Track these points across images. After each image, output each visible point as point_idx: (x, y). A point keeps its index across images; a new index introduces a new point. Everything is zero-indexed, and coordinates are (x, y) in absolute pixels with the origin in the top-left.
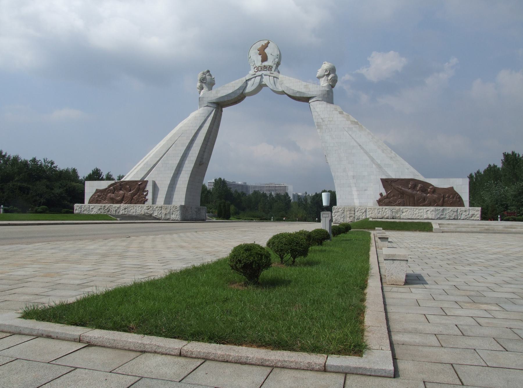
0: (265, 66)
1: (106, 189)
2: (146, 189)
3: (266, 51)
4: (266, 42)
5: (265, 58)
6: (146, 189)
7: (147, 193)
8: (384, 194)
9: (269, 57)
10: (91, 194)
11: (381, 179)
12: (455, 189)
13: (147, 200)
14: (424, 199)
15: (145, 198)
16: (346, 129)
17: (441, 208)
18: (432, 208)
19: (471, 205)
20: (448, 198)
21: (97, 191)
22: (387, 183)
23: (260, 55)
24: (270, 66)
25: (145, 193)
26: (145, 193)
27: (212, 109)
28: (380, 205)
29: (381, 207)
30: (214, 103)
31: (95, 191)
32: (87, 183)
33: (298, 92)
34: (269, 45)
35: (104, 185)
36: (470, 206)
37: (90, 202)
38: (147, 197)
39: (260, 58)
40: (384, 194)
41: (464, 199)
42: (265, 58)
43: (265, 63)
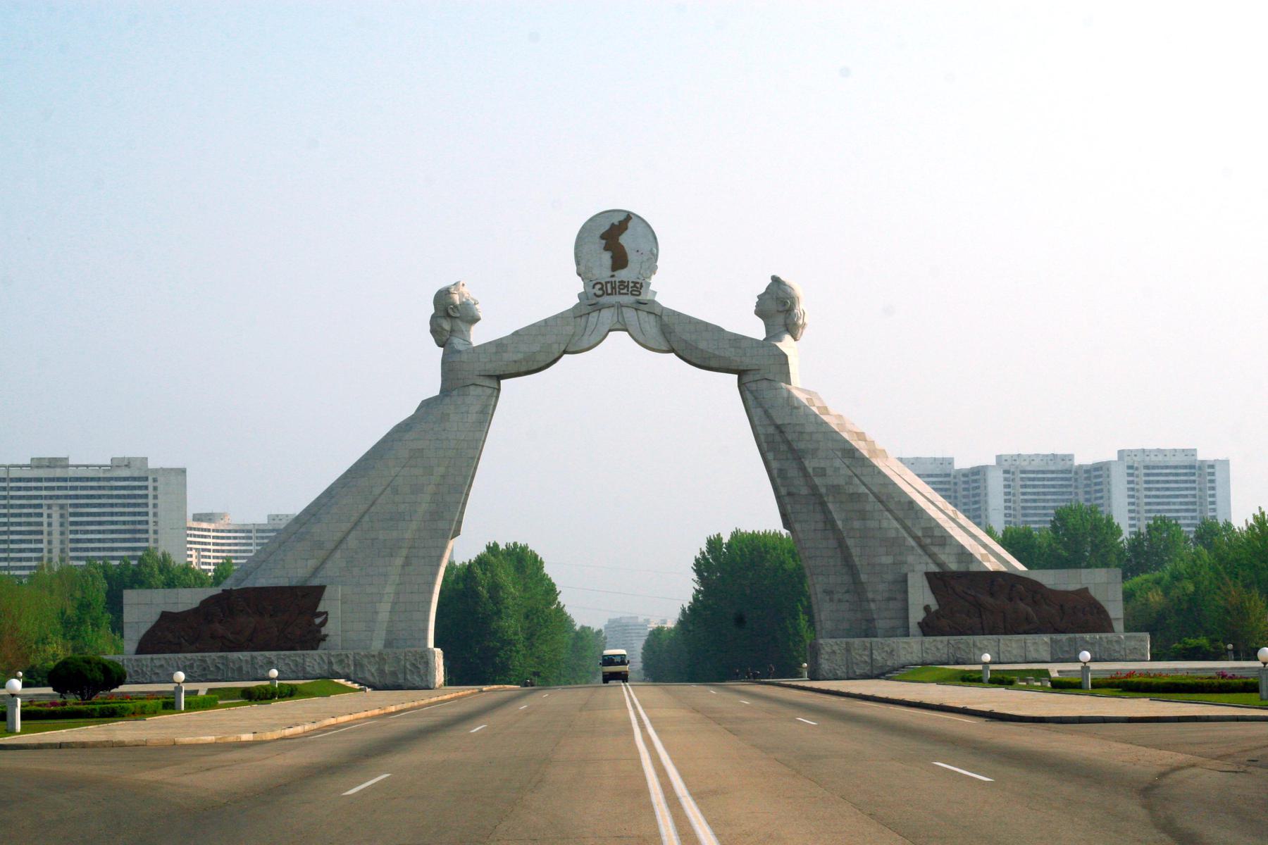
0: (622, 282)
1: (195, 612)
2: (320, 609)
3: (625, 240)
4: (622, 217)
5: (620, 261)
6: (320, 609)
7: (326, 620)
8: (934, 606)
9: (632, 256)
10: (144, 629)
11: (928, 575)
12: (1092, 592)
13: (324, 638)
14: (1028, 619)
15: (319, 631)
16: (839, 454)
17: (1064, 637)
18: (1046, 638)
19: (1132, 625)
20: (1080, 616)
21: (165, 616)
22: (939, 581)
23: (606, 248)
24: (635, 283)
25: (318, 621)
26: (318, 621)
27: (489, 391)
28: (925, 635)
29: (931, 639)
30: (490, 376)
31: (155, 617)
32: (129, 596)
33: (715, 356)
34: (630, 224)
35: (186, 599)
36: (1128, 629)
37: (140, 650)
38: (324, 631)
39: (607, 258)
40: (934, 606)
41: (1112, 615)
42: (620, 261)
43: (623, 275)
